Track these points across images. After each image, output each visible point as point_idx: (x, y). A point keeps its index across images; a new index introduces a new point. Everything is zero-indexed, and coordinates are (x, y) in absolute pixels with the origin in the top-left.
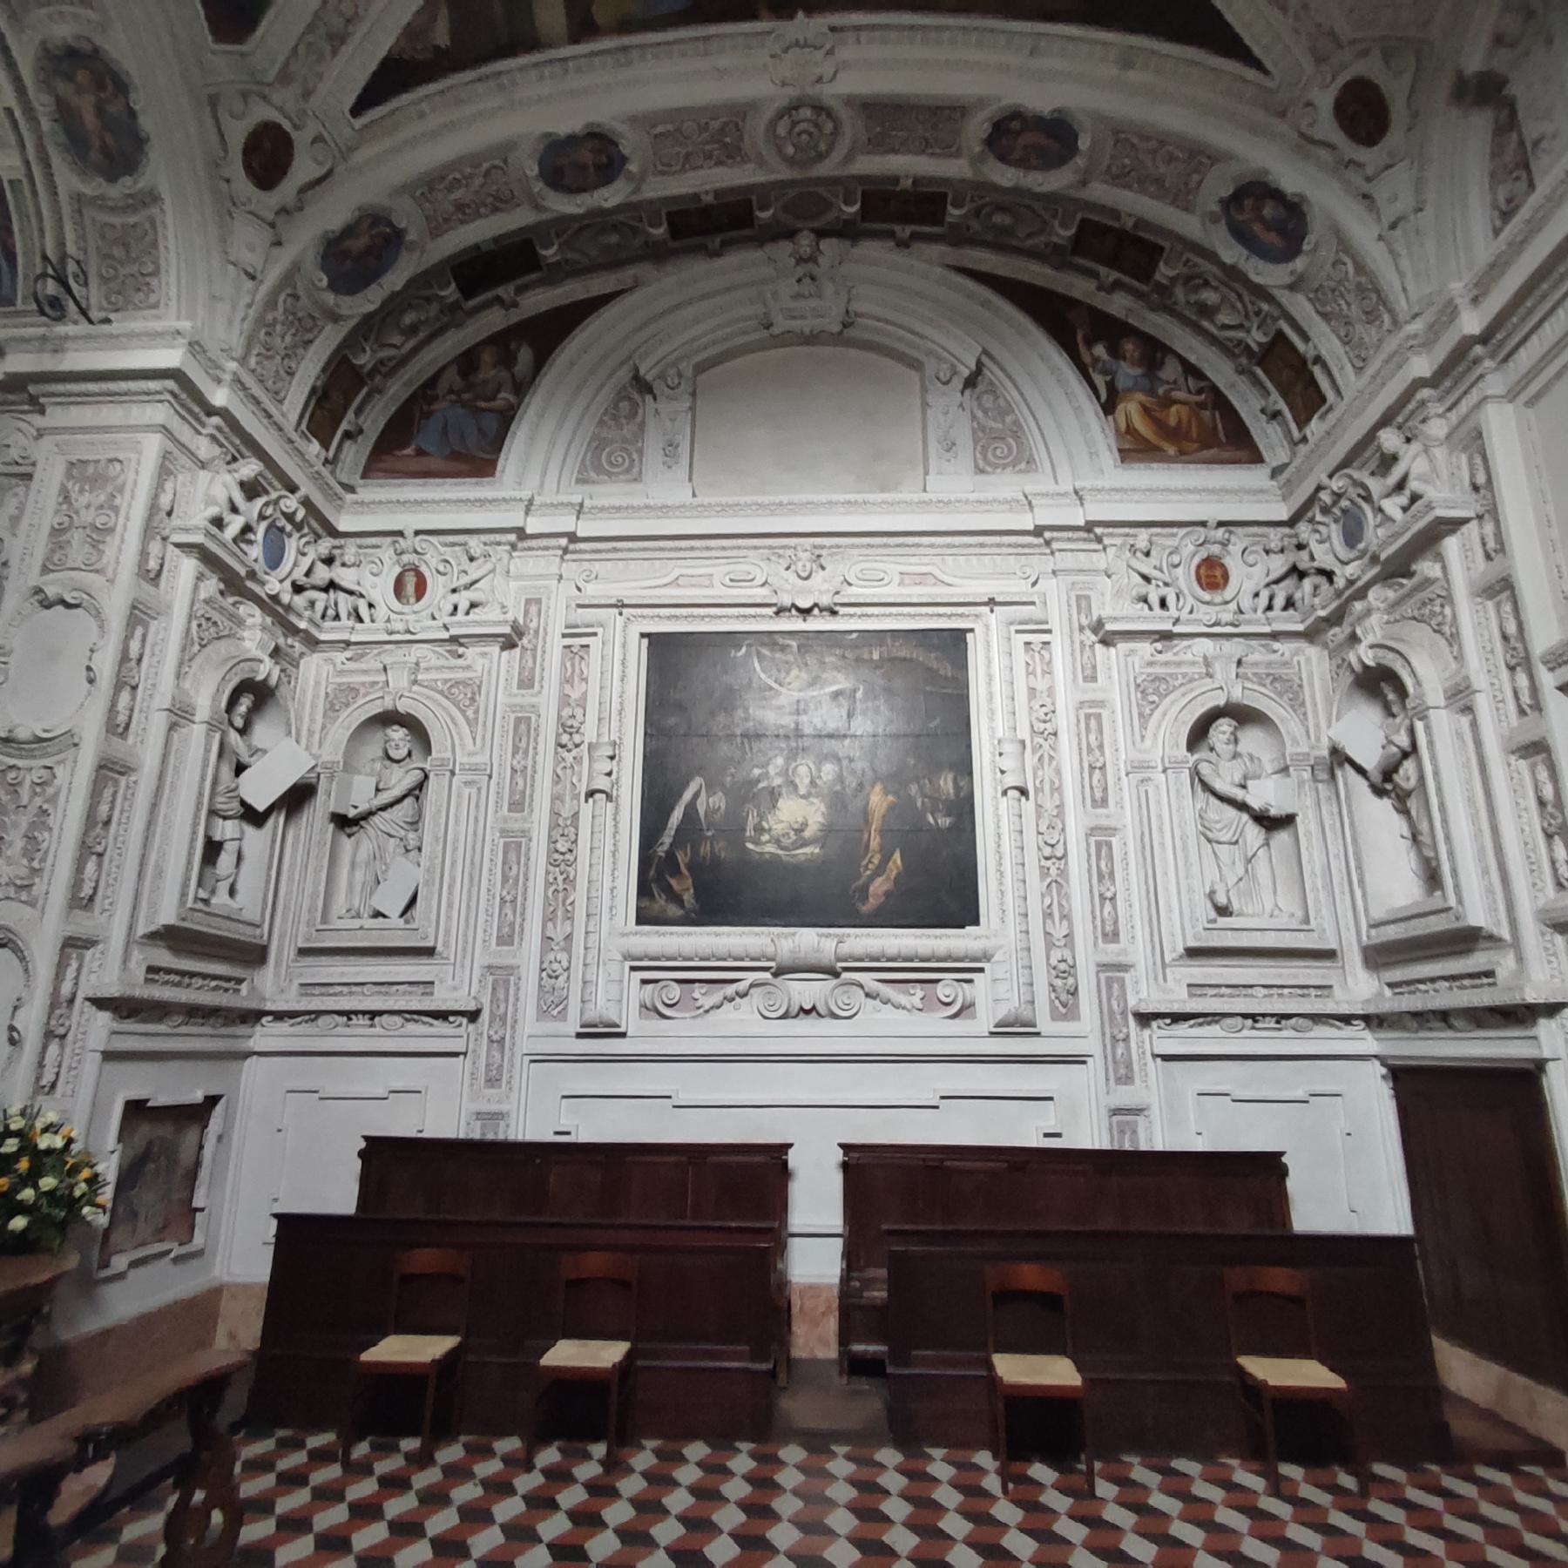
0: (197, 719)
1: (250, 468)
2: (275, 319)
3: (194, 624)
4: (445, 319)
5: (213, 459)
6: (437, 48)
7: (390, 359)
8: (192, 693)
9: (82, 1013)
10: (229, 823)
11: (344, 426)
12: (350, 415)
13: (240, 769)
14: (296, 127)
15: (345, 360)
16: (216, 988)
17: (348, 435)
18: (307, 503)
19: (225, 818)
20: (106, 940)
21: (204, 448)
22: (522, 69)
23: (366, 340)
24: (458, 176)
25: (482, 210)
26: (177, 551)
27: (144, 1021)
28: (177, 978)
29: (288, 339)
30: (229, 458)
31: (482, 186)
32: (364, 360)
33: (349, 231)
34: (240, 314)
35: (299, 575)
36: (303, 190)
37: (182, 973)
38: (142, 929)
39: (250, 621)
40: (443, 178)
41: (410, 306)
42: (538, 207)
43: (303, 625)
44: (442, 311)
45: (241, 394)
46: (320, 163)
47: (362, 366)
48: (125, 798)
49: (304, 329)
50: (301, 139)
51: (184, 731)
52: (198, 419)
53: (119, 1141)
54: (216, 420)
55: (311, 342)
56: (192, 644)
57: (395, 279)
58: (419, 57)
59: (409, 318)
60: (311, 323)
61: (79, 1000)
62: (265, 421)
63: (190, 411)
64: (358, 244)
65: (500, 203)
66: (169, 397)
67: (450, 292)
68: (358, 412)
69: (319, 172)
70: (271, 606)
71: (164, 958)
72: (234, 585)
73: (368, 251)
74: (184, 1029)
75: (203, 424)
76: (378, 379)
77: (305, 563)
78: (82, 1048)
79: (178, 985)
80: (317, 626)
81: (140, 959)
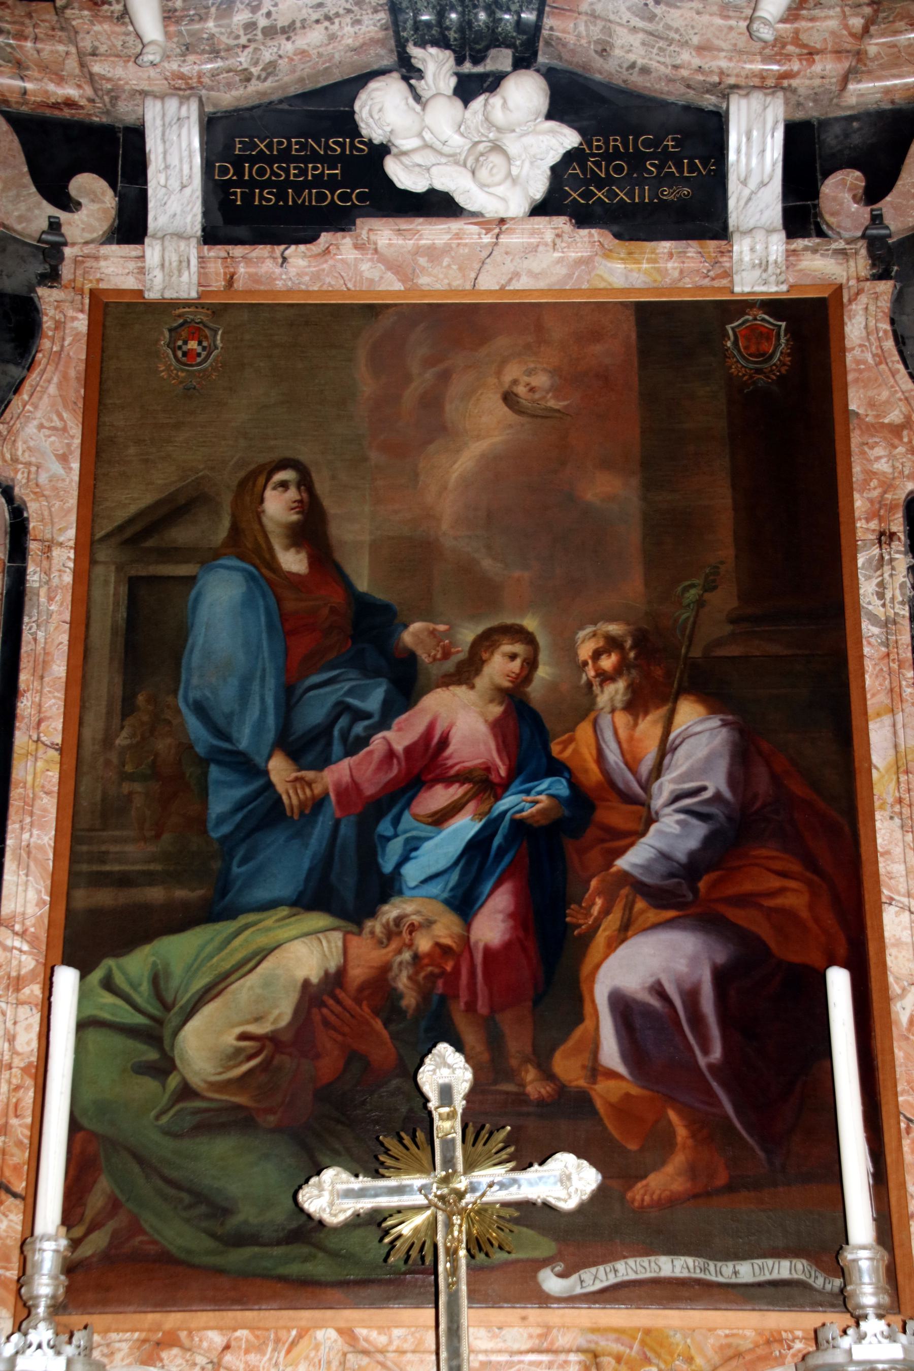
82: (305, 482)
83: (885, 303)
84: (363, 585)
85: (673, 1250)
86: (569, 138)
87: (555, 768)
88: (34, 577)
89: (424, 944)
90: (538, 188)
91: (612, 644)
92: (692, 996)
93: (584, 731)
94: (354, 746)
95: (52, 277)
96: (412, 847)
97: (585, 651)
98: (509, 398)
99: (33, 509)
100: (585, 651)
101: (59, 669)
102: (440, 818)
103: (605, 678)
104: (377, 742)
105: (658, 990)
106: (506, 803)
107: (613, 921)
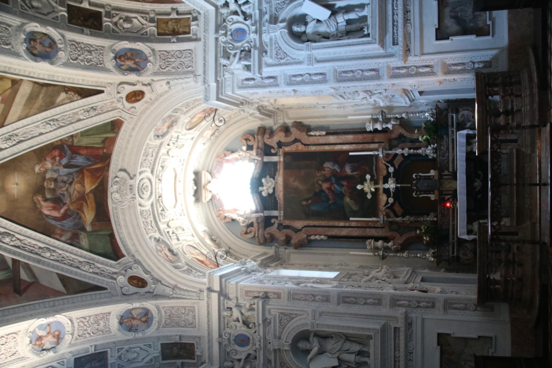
0: (310, 53)
1: (224, 61)
2: (173, 68)
3: (282, 61)
4: (113, 12)
5: (229, 73)
6: (67, 93)
7: (143, 17)
8: (303, 56)
9: (409, 63)
10: (339, 21)
11: (176, 17)
12: (171, 17)
13: (318, 21)
14: (122, 98)
15: (159, 34)
16: (397, 6)
17: (178, 13)
18: (217, 31)
19: (338, 23)
20: (387, 62)
21: (227, 75)
22: (44, 79)
23: (146, 32)
24: (86, 63)
25: (83, 46)
26: (263, 73)
27: (410, 43)
28: (395, 28)
29: (173, 60)
30: (225, 67)
31: (79, 55)
32: (152, 28)
33: (131, 70)
34: (181, 81)
35: (241, 18)
36: (134, 85)
37: (393, 25)
38: (381, 51)
39: (268, 37)
40: (91, 65)
41: (124, 28)
42: (63, 36)
43: (257, 11)
44: (113, 17)
45: (207, 78)
46: (123, 87)
47: (154, 26)
48: (343, 68)
49: (166, 56)
50: (124, 95)
51: (316, 55)
52: (222, 83)
53: (448, 39)
54: (219, 79)
55: (166, 51)
56: (288, 60)
57: (126, 45)
58: (73, 93)
59: (127, 26)
60: (161, 56)
61: (406, 65)
62: (206, 64)
63: (222, 87)
64: (130, 63)
65: (75, 44)
66: (224, 94)
67: (107, 22)
68: (169, 14)
69: (126, 86)
70: (258, 32)
71: (389, 38)
72: (263, 51)
73: (129, 59)
74: (412, 21)
75: (222, 80)
76: (152, 15)
77: (235, 17)
78: (419, 61)
79: (397, 27)
80: (254, 5)
81: (391, 49)
82: (302, 201)
83: (284, 147)
84: (312, 195)
85: (373, 168)
86: (268, 177)
87: (330, 177)
88: (312, 225)
89: (346, 189)
90: (272, 179)
91: (318, 172)
92: (351, 166)
93: (327, 175)
94: (328, 195)
95: (282, 224)
96: (338, 190)
97: (319, 175)
98: (294, 182)
99: (305, 225)
100: (319, 175)
101: (321, 222)
102: (334, 187)
103: (321, 173)
104: (328, 193)
105: (351, 169)
106: (333, 182)
107: (345, 173)
